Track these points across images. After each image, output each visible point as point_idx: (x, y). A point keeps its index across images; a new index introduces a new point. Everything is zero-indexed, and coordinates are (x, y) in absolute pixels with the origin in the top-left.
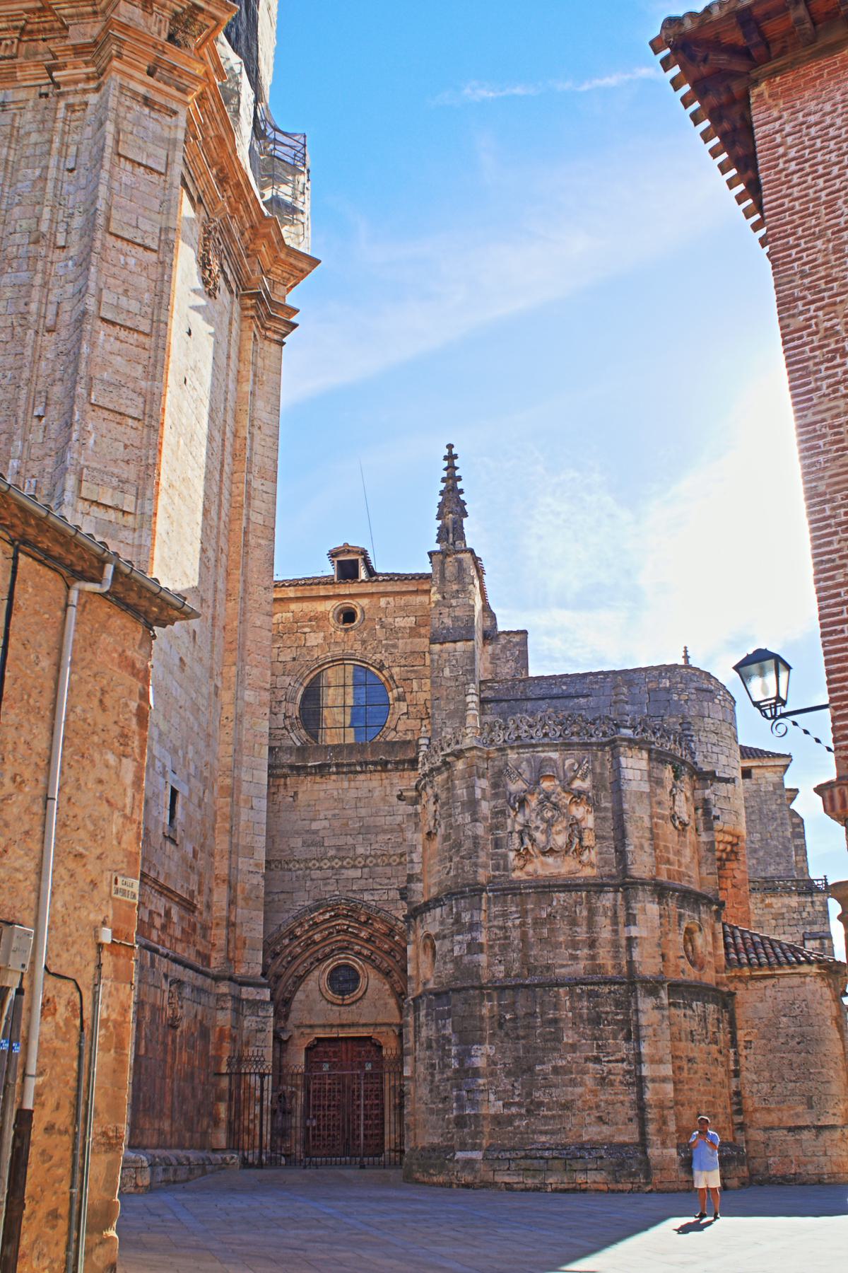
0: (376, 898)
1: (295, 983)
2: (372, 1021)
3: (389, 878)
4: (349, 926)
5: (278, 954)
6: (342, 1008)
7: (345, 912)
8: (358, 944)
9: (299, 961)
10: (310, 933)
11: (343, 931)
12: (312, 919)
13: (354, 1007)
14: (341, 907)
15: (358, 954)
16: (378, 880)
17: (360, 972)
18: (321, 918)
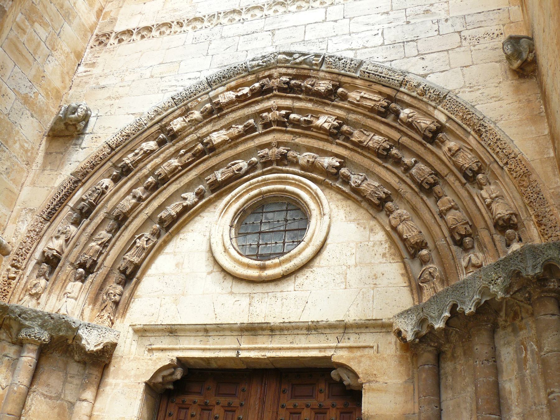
0: (354, 46)
1: (157, 234)
2: (333, 319)
3: (387, 13)
4: (292, 110)
5: (126, 171)
6: (259, 289)
7: (285, 79)
8: (309, 149)
9: (173, 188)
10: (204, 130)
11: (279, 123)
12: (210, 100)
13: (289, 286)
14: (275, 72)
15: (312, 167)
16: (360, 19)
17: (312, 205)
18: (232, 95)
